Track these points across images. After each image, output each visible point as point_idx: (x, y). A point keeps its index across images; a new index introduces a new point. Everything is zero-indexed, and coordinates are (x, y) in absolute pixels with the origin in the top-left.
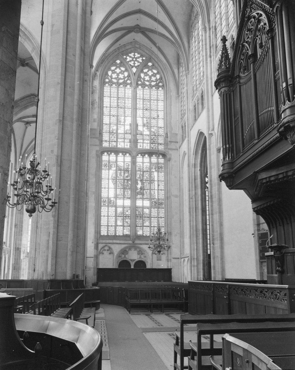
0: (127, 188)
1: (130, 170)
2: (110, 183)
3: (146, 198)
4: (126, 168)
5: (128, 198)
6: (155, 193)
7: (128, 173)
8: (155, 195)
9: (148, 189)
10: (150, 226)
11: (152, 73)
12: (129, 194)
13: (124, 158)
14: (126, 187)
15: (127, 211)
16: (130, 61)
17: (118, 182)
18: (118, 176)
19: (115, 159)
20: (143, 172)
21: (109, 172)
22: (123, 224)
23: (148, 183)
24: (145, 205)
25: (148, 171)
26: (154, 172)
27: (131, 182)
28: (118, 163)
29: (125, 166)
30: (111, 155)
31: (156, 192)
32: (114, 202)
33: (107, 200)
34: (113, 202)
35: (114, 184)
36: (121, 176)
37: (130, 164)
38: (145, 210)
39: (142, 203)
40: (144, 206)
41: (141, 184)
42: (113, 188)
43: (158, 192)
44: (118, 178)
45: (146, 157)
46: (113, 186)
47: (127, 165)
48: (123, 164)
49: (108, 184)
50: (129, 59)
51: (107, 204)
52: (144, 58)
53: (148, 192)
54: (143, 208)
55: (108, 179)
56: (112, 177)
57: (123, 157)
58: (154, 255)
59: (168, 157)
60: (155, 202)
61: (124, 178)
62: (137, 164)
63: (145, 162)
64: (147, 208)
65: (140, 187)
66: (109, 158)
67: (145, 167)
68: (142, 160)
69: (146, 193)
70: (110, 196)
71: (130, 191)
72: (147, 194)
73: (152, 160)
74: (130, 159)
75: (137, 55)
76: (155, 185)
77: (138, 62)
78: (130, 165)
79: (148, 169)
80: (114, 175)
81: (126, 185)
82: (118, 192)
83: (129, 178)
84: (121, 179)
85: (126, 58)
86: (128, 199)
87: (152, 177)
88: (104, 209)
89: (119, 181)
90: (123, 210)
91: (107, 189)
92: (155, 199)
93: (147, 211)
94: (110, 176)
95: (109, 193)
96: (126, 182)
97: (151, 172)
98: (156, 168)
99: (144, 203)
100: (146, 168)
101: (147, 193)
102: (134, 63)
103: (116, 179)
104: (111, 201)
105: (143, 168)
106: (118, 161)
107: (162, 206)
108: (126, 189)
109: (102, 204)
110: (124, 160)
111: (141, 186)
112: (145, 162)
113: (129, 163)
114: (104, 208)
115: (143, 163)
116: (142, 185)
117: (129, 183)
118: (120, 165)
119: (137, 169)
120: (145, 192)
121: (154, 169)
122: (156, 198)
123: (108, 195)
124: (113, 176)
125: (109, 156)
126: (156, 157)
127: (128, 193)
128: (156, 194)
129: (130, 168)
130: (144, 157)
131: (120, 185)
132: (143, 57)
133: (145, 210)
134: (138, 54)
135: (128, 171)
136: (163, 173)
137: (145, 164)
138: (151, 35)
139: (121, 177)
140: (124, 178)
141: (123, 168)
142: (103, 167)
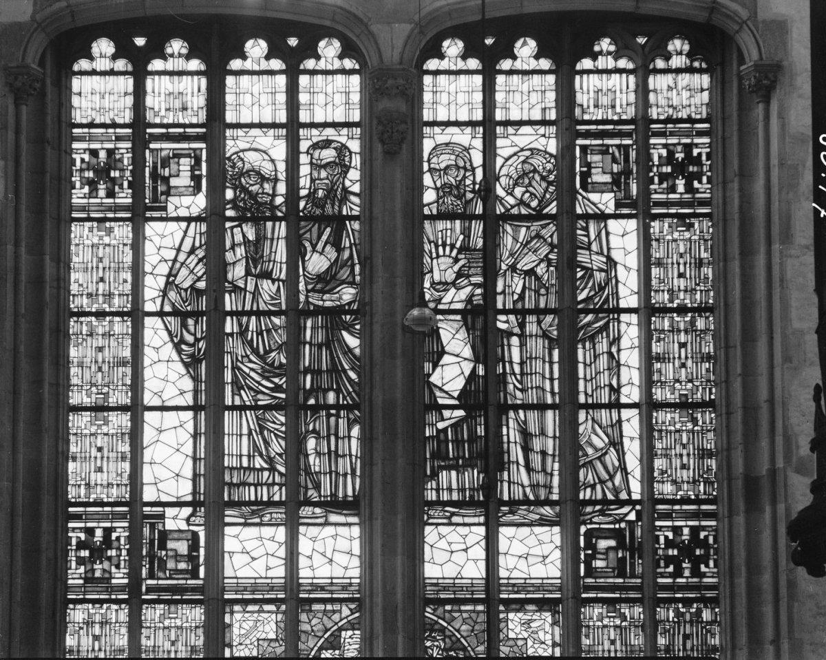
0: (331, 398)
1: (354, 206)
2: (149, 355)
3: (526, 502)
4: (311, 195)
5: (335, 504)
7: (339, 250)
8: (623, 468)
9: (542, 407)
12: (343, 465)
13: (292, 90)
14: (317, 390)
17: (234, 346)
18: (237, 272)
19: (199, 101)
20: (493, 223)
23: (545, 335)
24: (511, 568)
25: (538, 215)
26: (612, 224)
27: (361, 335)
28: (234, 143)
29: (305, 170)
30: (157, 65)
31: (632, 425)
32: (194, 546)
33: (121, 530)
34: (182, 547)
36: (267, 275)
37: (355, 146)
38: (514, 625)
39: (479, 552)
41: (467, 352)
42: (189, 400)
43: (649, 432)
44: (229, 303)
45: (518, 65)
46: (188, 384)
47: (329, 155)
48: (279, 151)
49: (136, 361)
51: (120, 578)
53: (543, 433)
55: (136, 315)
56: (172, 295)
57: (281, 80)
59: (752, 55)
60: (617, 534)
61: (293, 292)
62: (428, 145)
63: (515, 115)
64: (542, 604)
65: (457, 386)
66: (139, 93)
67: (506, 170)
68: (478, 97)
69: (527, 449)
70: (149, 495)
71: (355, 431)
72: (536, 460)
73: (587, 88)
74: (356, 98)
76: (624, 357)
78: (356, 161)
79: (539, 187)
80: (192, 274)
81: (316, 373)
83: (347, 294)
84: (259, 314)
86: (334, 518)
87: (589, 272)
88: (89, 623)
89: (243, 332)
91: (124, 420)
92: (622, 503)
94: (148, 280)
95: (147, 455)
96: (320, 337)
98: (627, 172)
99: (503, 545)
100: (523, 177)
101: (537, 444)
103: (217, 314)
104: (163, 546)
105: (491, 176)
106: (230, 117)
107: (696, 572)
108: (316, 409)
109: (76, 574)
110: (293, 105)
111: (467, 368)
112: (507, 123)
113: (342, 137)
114: (98, 613)
115: (489, 126)
116: (476, 359)
117: (348, 351)
119: (429, 196)
120: (511, 432)
121: (601, 188)
124: (184, 279)
125: (140, 75)
126: (623, 63)
127: (334, 455)
128: (633, 450)
129: (356, 188)
130: (506, 64)
135: (339, 222)
136: (707, 223)
137: (504, 147)
139: (267, 287)
140: (293, 292)
141: (282, 188)
142: (79, 196)
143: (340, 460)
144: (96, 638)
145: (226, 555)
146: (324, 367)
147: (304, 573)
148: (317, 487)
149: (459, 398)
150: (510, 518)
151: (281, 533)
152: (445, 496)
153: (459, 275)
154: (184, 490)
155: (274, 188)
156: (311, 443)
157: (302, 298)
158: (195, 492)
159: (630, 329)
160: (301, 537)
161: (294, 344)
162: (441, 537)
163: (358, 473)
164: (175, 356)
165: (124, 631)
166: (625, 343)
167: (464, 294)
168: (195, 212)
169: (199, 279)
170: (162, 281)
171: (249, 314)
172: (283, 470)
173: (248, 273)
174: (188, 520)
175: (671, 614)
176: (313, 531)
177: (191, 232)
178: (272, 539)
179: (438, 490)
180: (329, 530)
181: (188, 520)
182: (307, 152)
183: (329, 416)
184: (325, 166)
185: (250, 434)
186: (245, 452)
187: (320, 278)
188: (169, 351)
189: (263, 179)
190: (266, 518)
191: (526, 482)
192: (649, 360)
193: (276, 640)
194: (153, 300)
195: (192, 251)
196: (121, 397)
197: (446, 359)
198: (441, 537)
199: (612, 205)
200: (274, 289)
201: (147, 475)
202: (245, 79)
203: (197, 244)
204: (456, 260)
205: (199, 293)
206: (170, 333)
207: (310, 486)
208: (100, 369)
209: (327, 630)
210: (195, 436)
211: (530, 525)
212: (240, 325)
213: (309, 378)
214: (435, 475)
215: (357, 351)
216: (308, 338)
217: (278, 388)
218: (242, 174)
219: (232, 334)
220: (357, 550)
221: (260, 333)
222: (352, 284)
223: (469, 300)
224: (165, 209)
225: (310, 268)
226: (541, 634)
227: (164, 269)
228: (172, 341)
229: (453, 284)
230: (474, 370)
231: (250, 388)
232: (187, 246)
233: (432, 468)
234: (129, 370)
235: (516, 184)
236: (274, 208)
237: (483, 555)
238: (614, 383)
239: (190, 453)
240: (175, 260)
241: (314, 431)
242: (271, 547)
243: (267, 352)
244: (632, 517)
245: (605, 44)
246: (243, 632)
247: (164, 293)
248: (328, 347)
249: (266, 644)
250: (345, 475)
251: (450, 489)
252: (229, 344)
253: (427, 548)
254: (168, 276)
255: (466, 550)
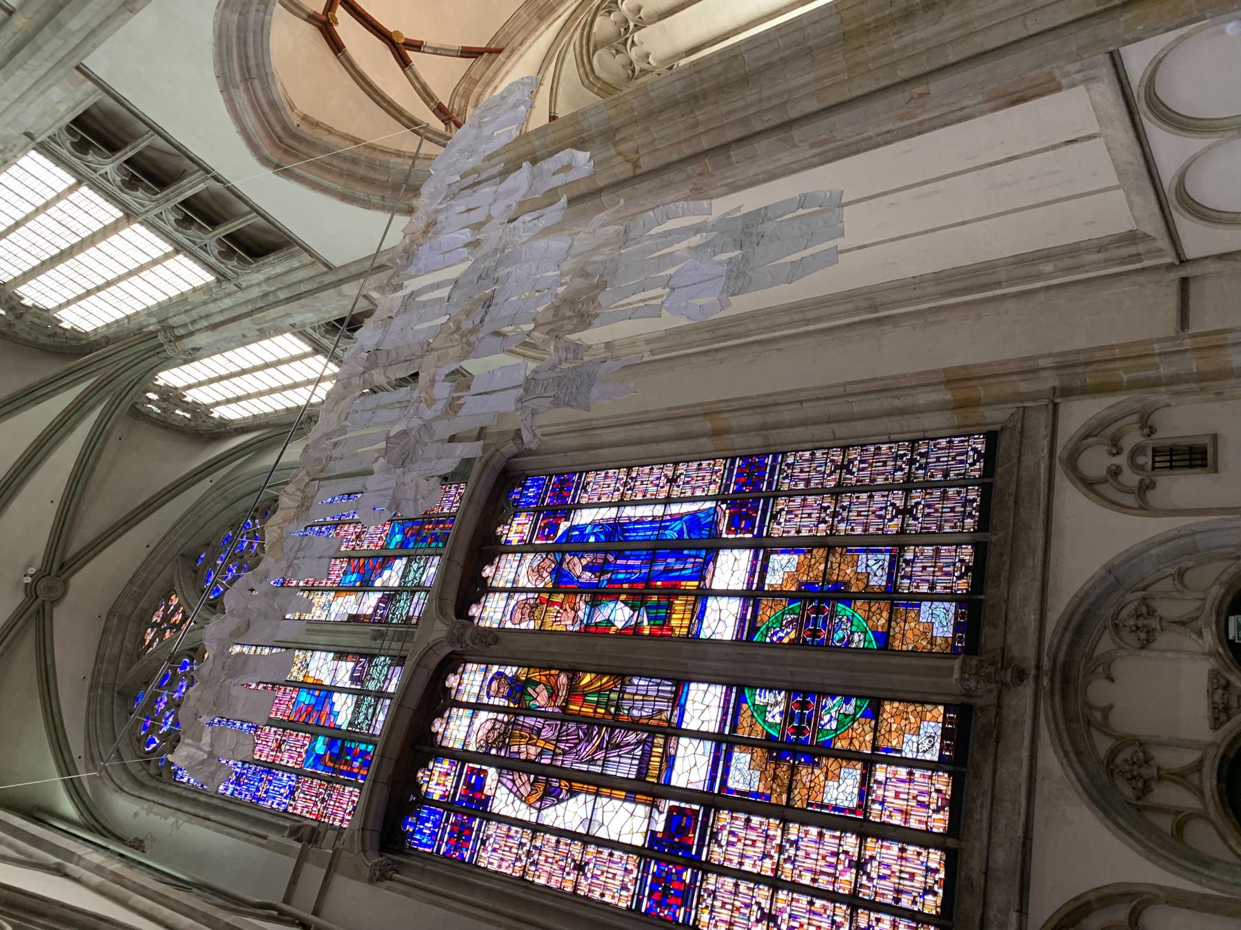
1: (523, 673)
2: (559, 824)
6: (679, 517)
7: (540, 683)
10: (896, 546)
15: (763, 710)
21: (501, 819)
22: (849, 756)
23: (616, 559)
27: (585, 672)
31: (675, 509)
35: (573, 793)
36: (540, 731)
37: (495, 669)
38: (774, 579)
39: (724, 601)
40: (750, 583)
41: (612, 605)
42: (590, 798)
46: (582, 797)
47: (495, 685)
48: (483, 715)
49: (560, 833)
54: (753, 596)
55: (537, 828)
56: (532, 800)
58: (1154, 497)
62: (509, 625)
65: (628, 612)
70: (638, 841)
71: (635, 681)
80: (524, 782)
82: (625, 768)
83: (563, 679)
86: (683, 701)
90: (748, 744)
93: (782, 569)
95: (614, 837)
97: (576, 541)
106: (458, 746)
108: (618, 708)
110: (467, 705)
111: (620, 605)
113: (490, 676)
116: (617, 600)
117: (591, 683)
118: (480, 734)
122: (713, 504)
123: (628, 849)
125: (426, 800)
129: (515, 669)
131: (586, 750)
133: (774, 579)
137: (523, 582)
138: (85, 533)
141: (501, 716)
143: (649, 693)
144: (723, 907)
145: (690, 786)
146: (596, 699)
147: (713, 727)
148: (661, 711)
149: (634, 611)
150: (707, 582)
151: (684, 741)
152: (686, 622)
153: (573, 609)
154: (642, 810)
155: (499, 721)
156: (635, 713)
157: (557, 710)
158: (645, 804)
159: (629, 512)
160: (689, 728)
161: (579, 719)
162: (709, 627)
163: (659, 681)
164: (564, 804)
165: (721, 879)
166: (632, 514)
167: (582, 605)
168: (496, 776)
169: (529, 779)
170: (524, 806)
171: (556, 746)
172: (646, 735)
173: (534, 745)
174: (661, 813)
175: (787, 481)
176: (687, 717)
177: (504, 780)
178: (686, 748)
179: (681, 627)
180: (689, 706)
181: (661, 813)
182: (489, 698)
183: (623, 699)
184: (499, 688)
185: (619, 756)
186: (629, 761)
187: (550, 697)
188: (560, 808)
189: (493, 728)
190: (672, 751)
191: (690, 571)
192: (645, 502)
193: (752, 754)
194: (531, 814)
195: (513, 781)
196: (576, 848)
197: (611, 618)
198: (709, 627)
199: (566, 523)
200: (547, 727)
201: (625, 839)
202: (448, 733)
203: (511, 777)
204: (566, 610)
205: (536, 780)
206: (551, 806)
207: (659, 717)
208: (557, 862)
209: (752, 716)
210: (611, 797)
211: (715, 568)
212: (560, 754)
213: (599, 710)
214: (672, 629)
215: (593, 675)
216: (578, 708)
217: (599, 733)
218: (486, 742)
219: (563, 761)
220: (704, 686)
221: (567, 742)
222: (559, 676)
223: (586, 603)
224: (488, 797)
225: (543, 703)
226: (784, 562)
227: (517, 802)
228: (555, 805)
229: (576, 612)
230: (622, 601)
231: (595, 752)
232: (510, 784)
233: (669, 630)
234: (563, 840)
235: (541, 576)
236: (508, 723)
237: (725, 599)
238: (650, 519)
239: (620, 803)
240: (515, 795)
241: (629, 710)
242: (691, 750)
243: (578, 738)
244: (724, 506)
245: (500, 529)
246: (741, 781)
247: (530, 806)
248: (586, 695)
249: (753, 763)
250: (658, 691)
251: (682, 619)
252: (567, 765)
253: (713, 637)
254: (521, 800)
255: (720, 610)
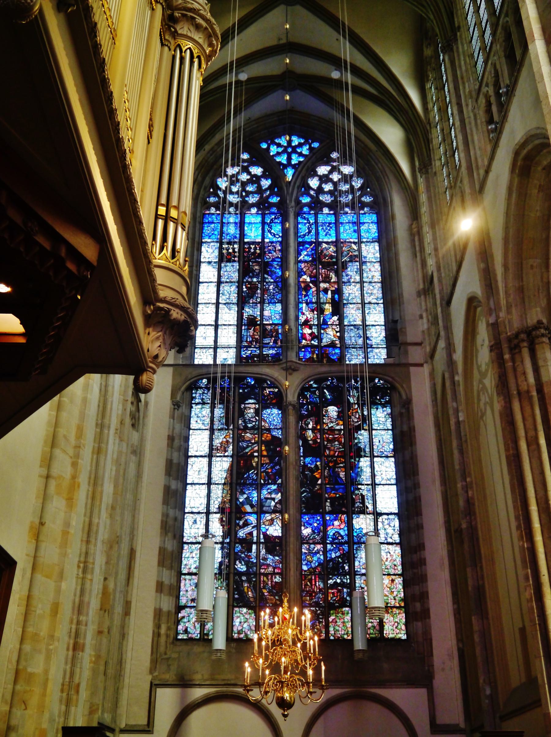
11: (340, 177)
16: (278, 154)
50: (274, 150)
52: (316, 145)
75: (296, 141)
77: (300, 154)
85: (268, 149)
102: (289, 159)
132: (313, 142)
134: (299, 137)
